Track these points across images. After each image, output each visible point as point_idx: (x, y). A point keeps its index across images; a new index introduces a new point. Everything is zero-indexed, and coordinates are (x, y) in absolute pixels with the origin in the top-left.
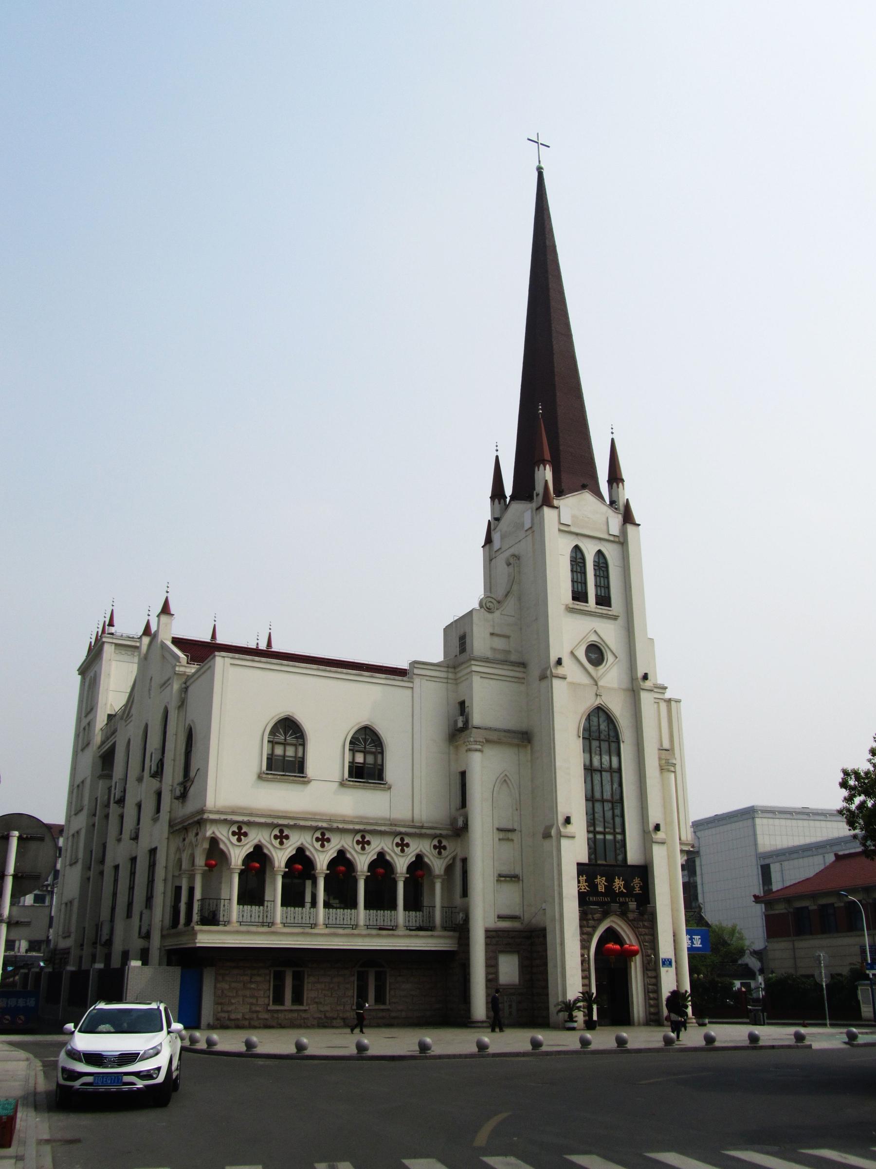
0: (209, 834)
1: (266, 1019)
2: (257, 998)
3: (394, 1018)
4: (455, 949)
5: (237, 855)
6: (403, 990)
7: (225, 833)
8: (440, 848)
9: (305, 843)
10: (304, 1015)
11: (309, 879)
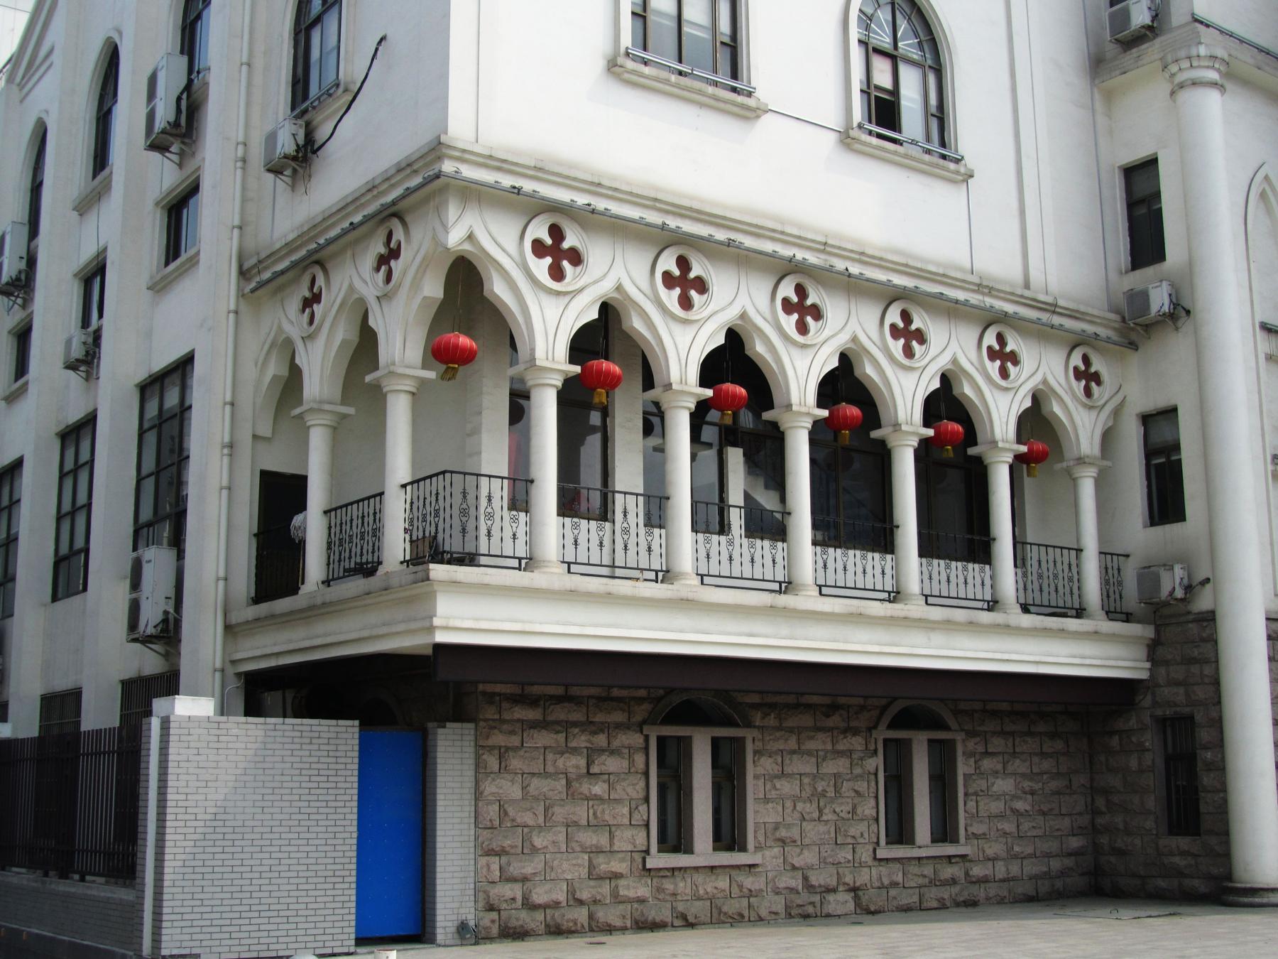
0: (455, 238)
1: (641, 901)
2: (611, 829)
3: (984, 880)
4: (1143, 675)
5: (551, 326)
6: (1000, 797)
7: (510, 243)
8: (1088, 376)
9: (752, 313)
10: (749, 882)
11: (735, 445)
